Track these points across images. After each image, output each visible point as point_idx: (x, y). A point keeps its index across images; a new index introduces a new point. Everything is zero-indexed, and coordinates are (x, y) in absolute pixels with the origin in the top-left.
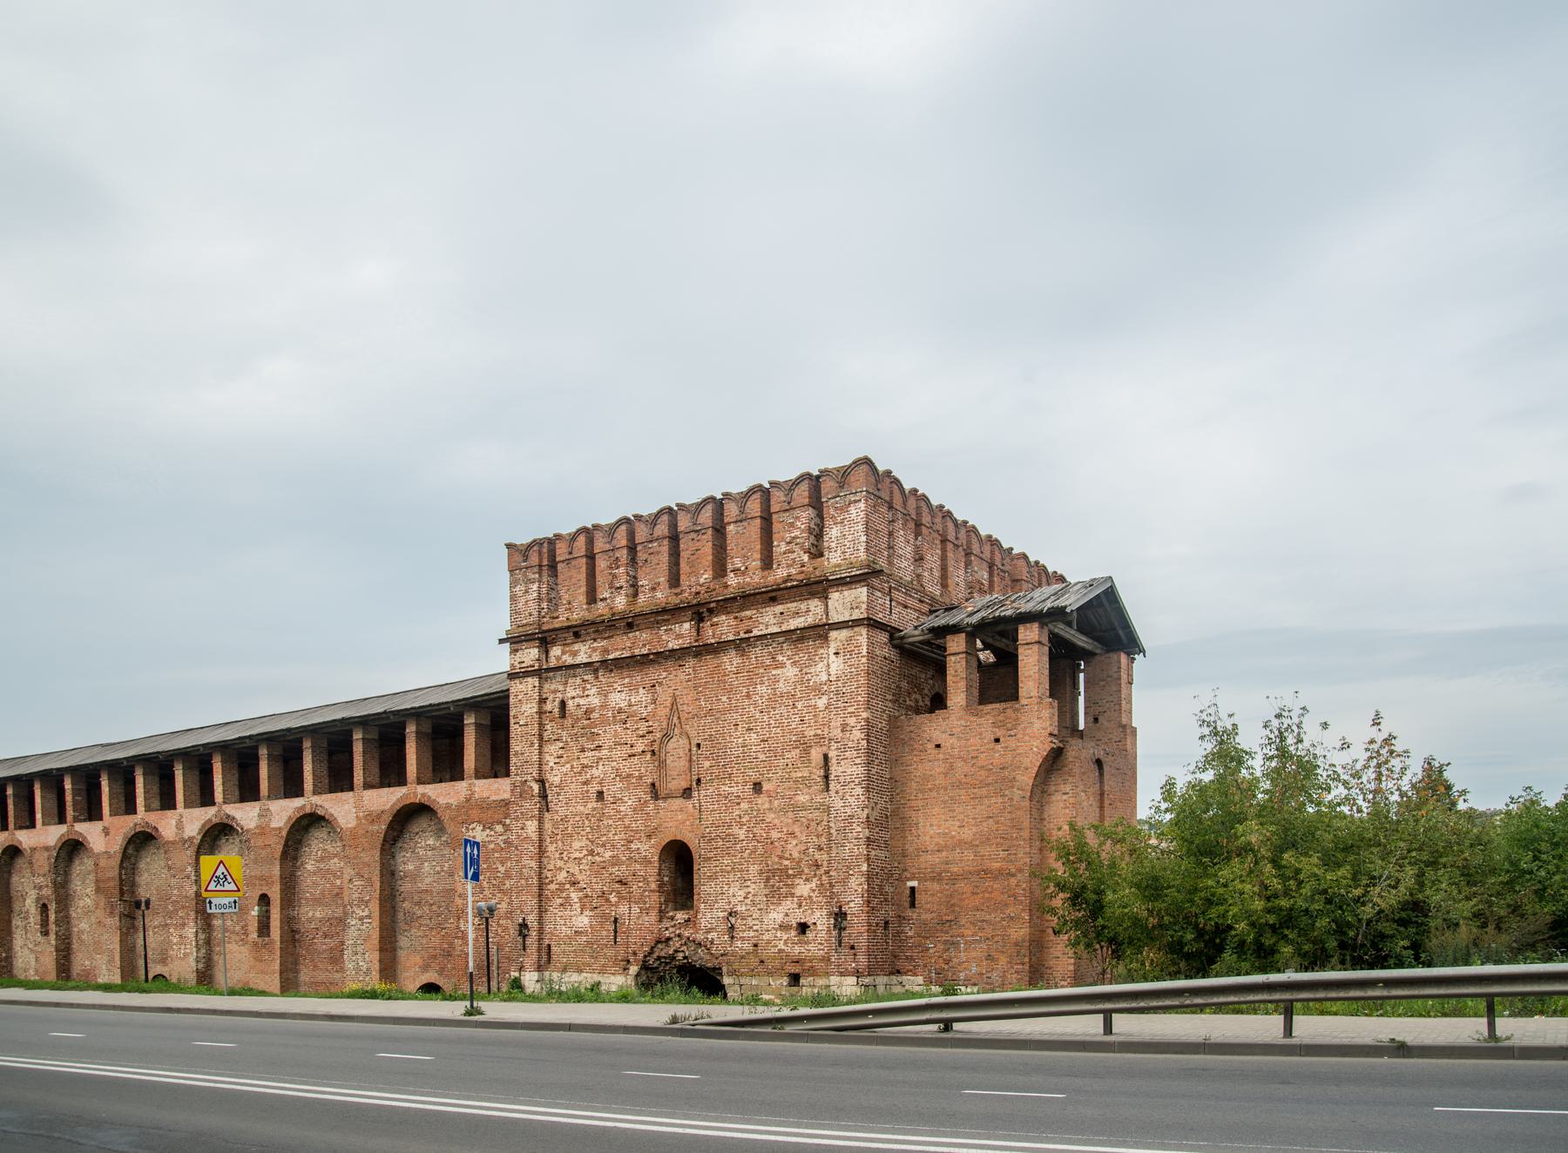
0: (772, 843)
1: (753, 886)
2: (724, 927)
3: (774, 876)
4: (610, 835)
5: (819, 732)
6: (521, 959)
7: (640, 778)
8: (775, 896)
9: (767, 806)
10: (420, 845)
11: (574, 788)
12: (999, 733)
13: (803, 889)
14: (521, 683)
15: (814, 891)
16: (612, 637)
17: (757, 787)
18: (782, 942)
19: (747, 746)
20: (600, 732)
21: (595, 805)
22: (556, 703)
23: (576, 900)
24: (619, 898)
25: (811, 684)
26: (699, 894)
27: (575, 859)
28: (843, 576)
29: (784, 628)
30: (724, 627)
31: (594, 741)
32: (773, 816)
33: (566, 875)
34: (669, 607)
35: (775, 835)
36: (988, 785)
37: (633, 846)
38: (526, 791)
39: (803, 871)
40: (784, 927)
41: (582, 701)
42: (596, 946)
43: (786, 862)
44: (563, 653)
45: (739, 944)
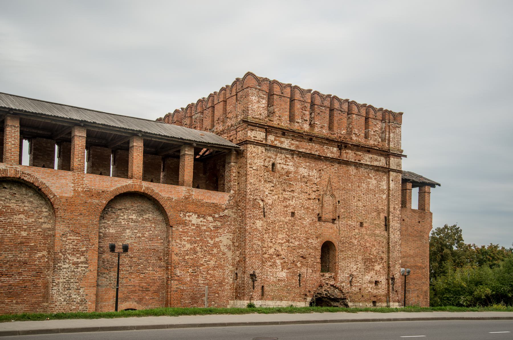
0: (367, 248)
1: (360, 264)
2: (348, 281)
3: (367, 261)
4: (298, 234)
5: (383, 208)
6: (251, 294)
7: (313, 210)
8: (368, 269)
9: (365, 232)
10: (122, 218)
11: (279, 208)
12: (420, 220)
13: (377, 267)
14: (254, 148)
15: (381, 268)
16: (301, 141)
17: (361, 224)
18: (370, 288)
19: (358, 207)
20: (294, 184)
21: (290, 218)
22: (271, 163)
23: (279, 264)
24: (303, 265)
25: (381, 189)
26: (338, 266)
27: (279, 243)
28: (395, 153)
29: (372, 164)
30: (350, 155)
31: (290, 187)
32: (367, 237)
33: (274, 251)
34: (330, 138)
35: (368, 245)
36: (417, 237)
37: (309, 241)
38: (256, 204)
39: (377, 260)
40: (370, 282)
41: (285, 167)
42: (289, 287)
43: (372, 256)
44: (275, 140)
45: (354, 288)
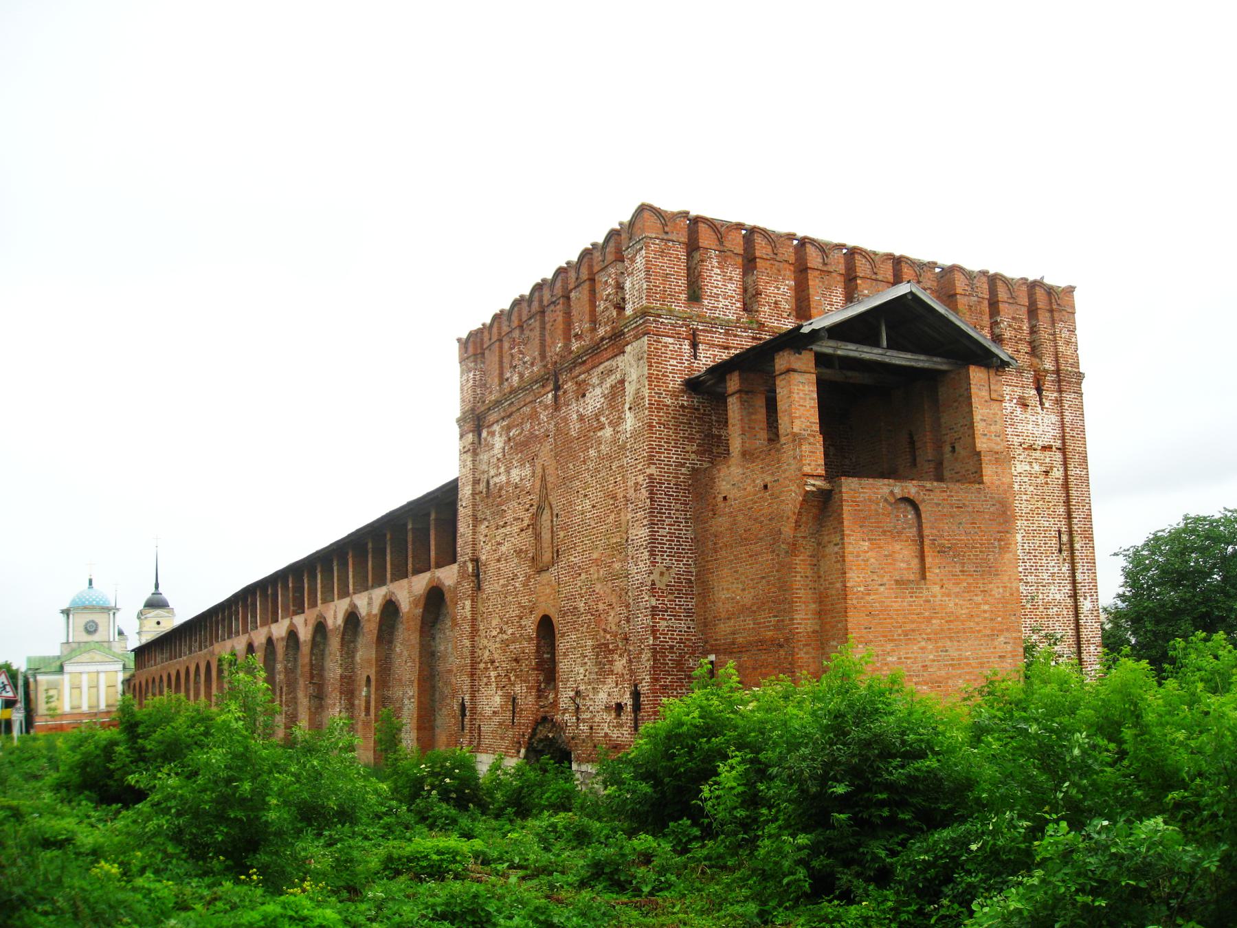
8: (603, 670)
12: (768, 479)
24: (517, 676)
35: (601, 606)
40: (608, 708)
43: (608, 636)
